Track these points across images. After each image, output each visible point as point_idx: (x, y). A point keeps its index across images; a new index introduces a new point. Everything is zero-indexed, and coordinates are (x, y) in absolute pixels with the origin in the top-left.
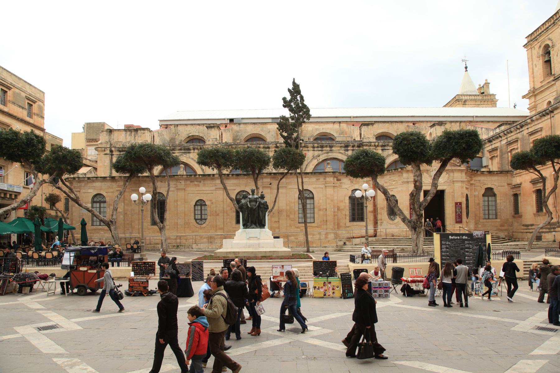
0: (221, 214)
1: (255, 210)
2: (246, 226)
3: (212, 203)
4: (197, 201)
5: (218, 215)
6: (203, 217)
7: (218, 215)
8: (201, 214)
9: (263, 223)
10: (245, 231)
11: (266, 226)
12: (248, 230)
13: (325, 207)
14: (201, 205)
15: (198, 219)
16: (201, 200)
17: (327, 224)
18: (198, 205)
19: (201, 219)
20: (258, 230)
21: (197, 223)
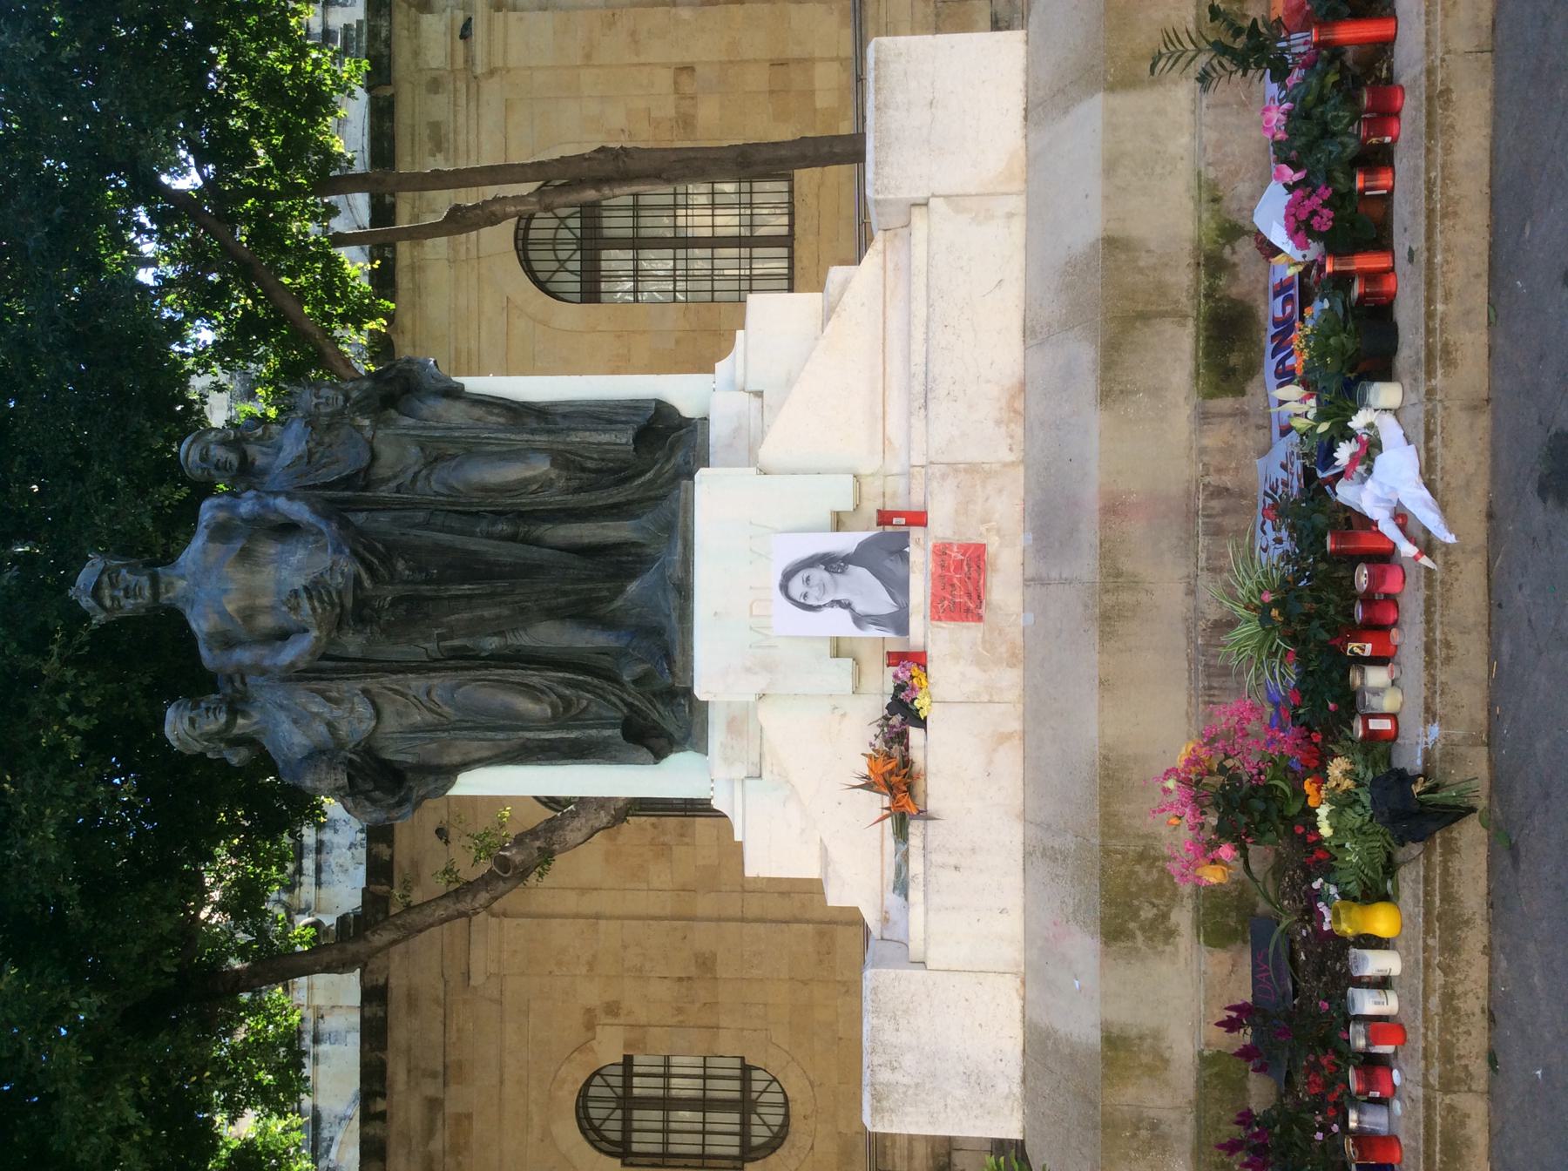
0: (703, 937)
1: (374, 554)
2: (657, 713)
3: (612, 1009)
4: (590, 1129)
5: (706, 963)
6: (728, 1089)
7: (706, 963)
8: (704, 1104)
9: (624, 438)
10: (735, 726)
11: (682, 392)
12: (714, 668)
13: (664, 79)
14: (628, 1102)
15: (744, 1133)
16: (583, 1098)
17: (806, 62)
18: (627, 1129)
19: (745, 1105)
20: (719, 505)
21: (778, 1139)
